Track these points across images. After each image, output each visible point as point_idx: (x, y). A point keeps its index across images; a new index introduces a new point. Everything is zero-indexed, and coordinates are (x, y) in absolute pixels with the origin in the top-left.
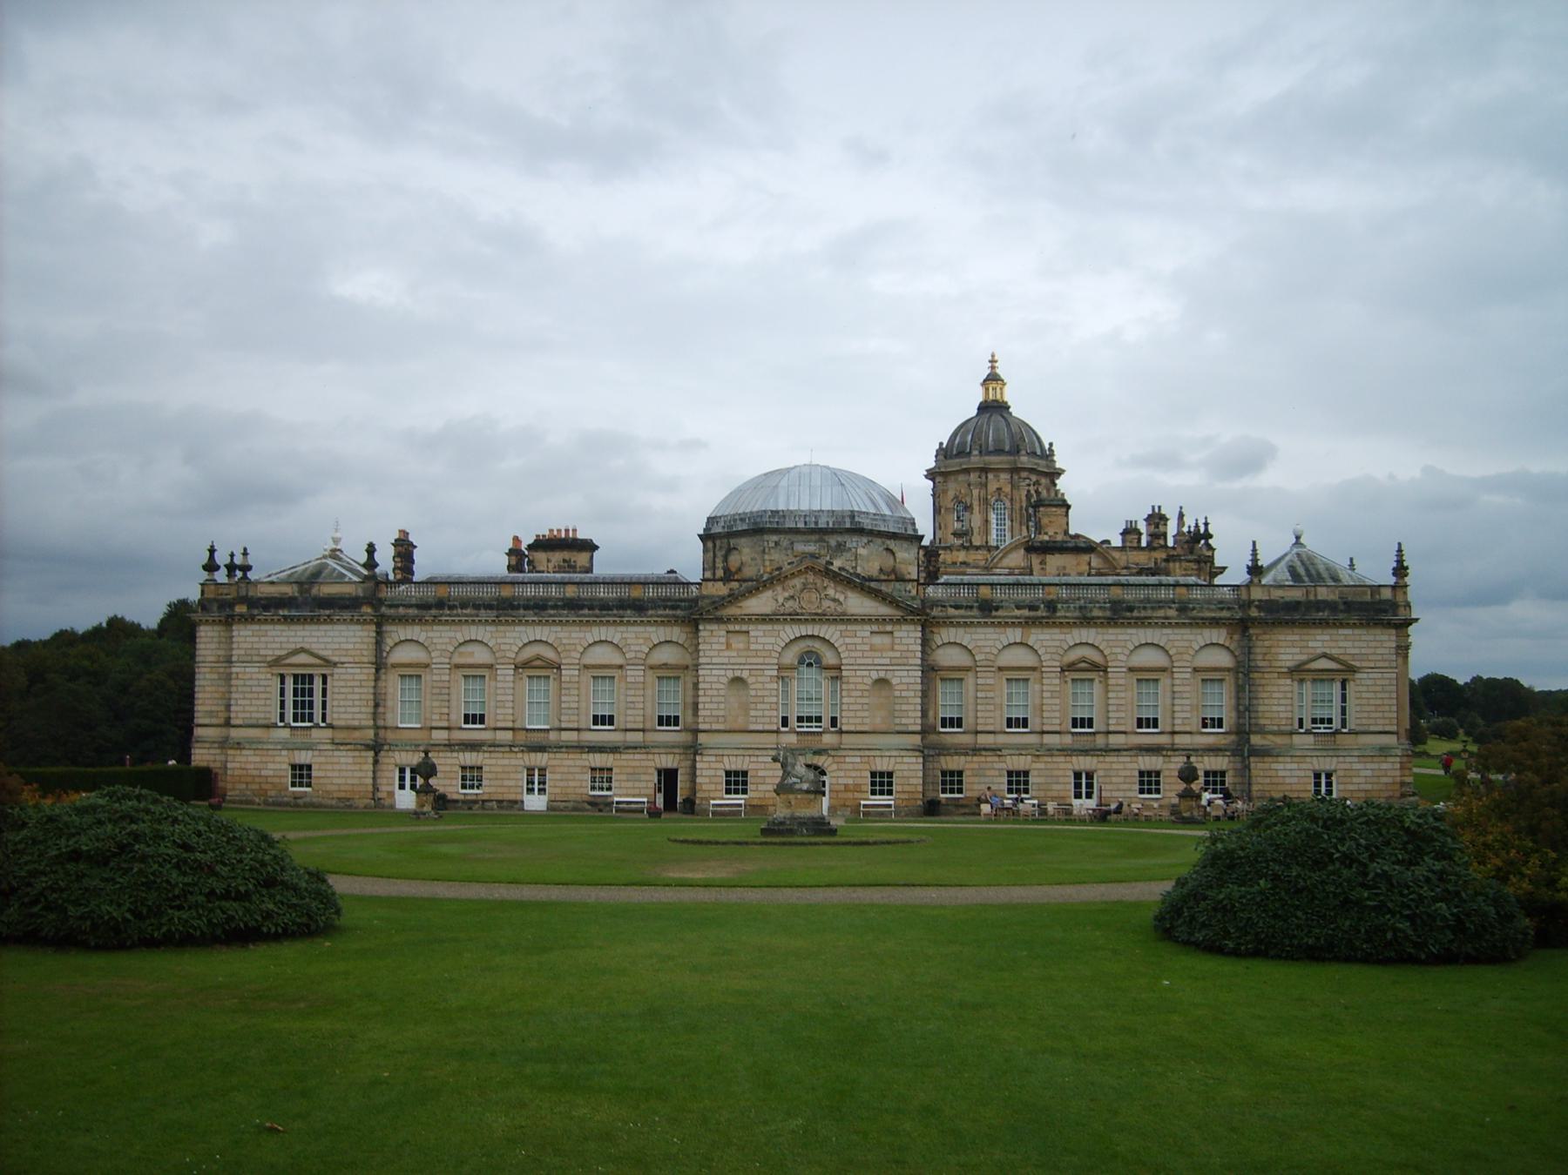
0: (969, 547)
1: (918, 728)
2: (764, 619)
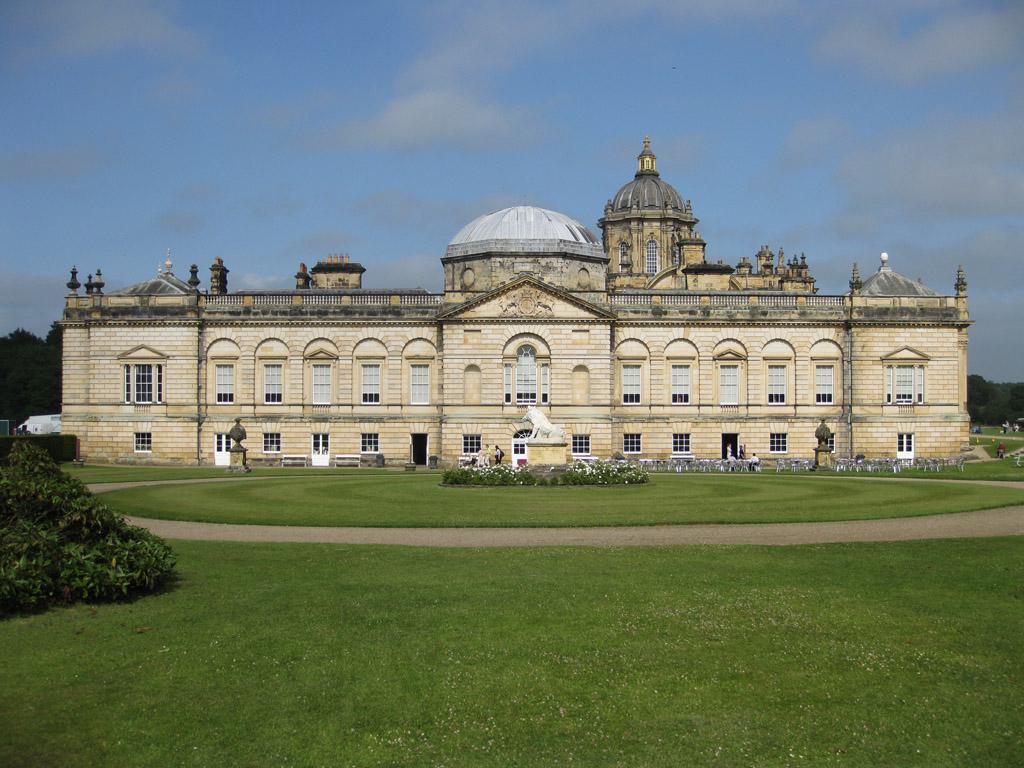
0: (630, 274)
1: (608, 402)
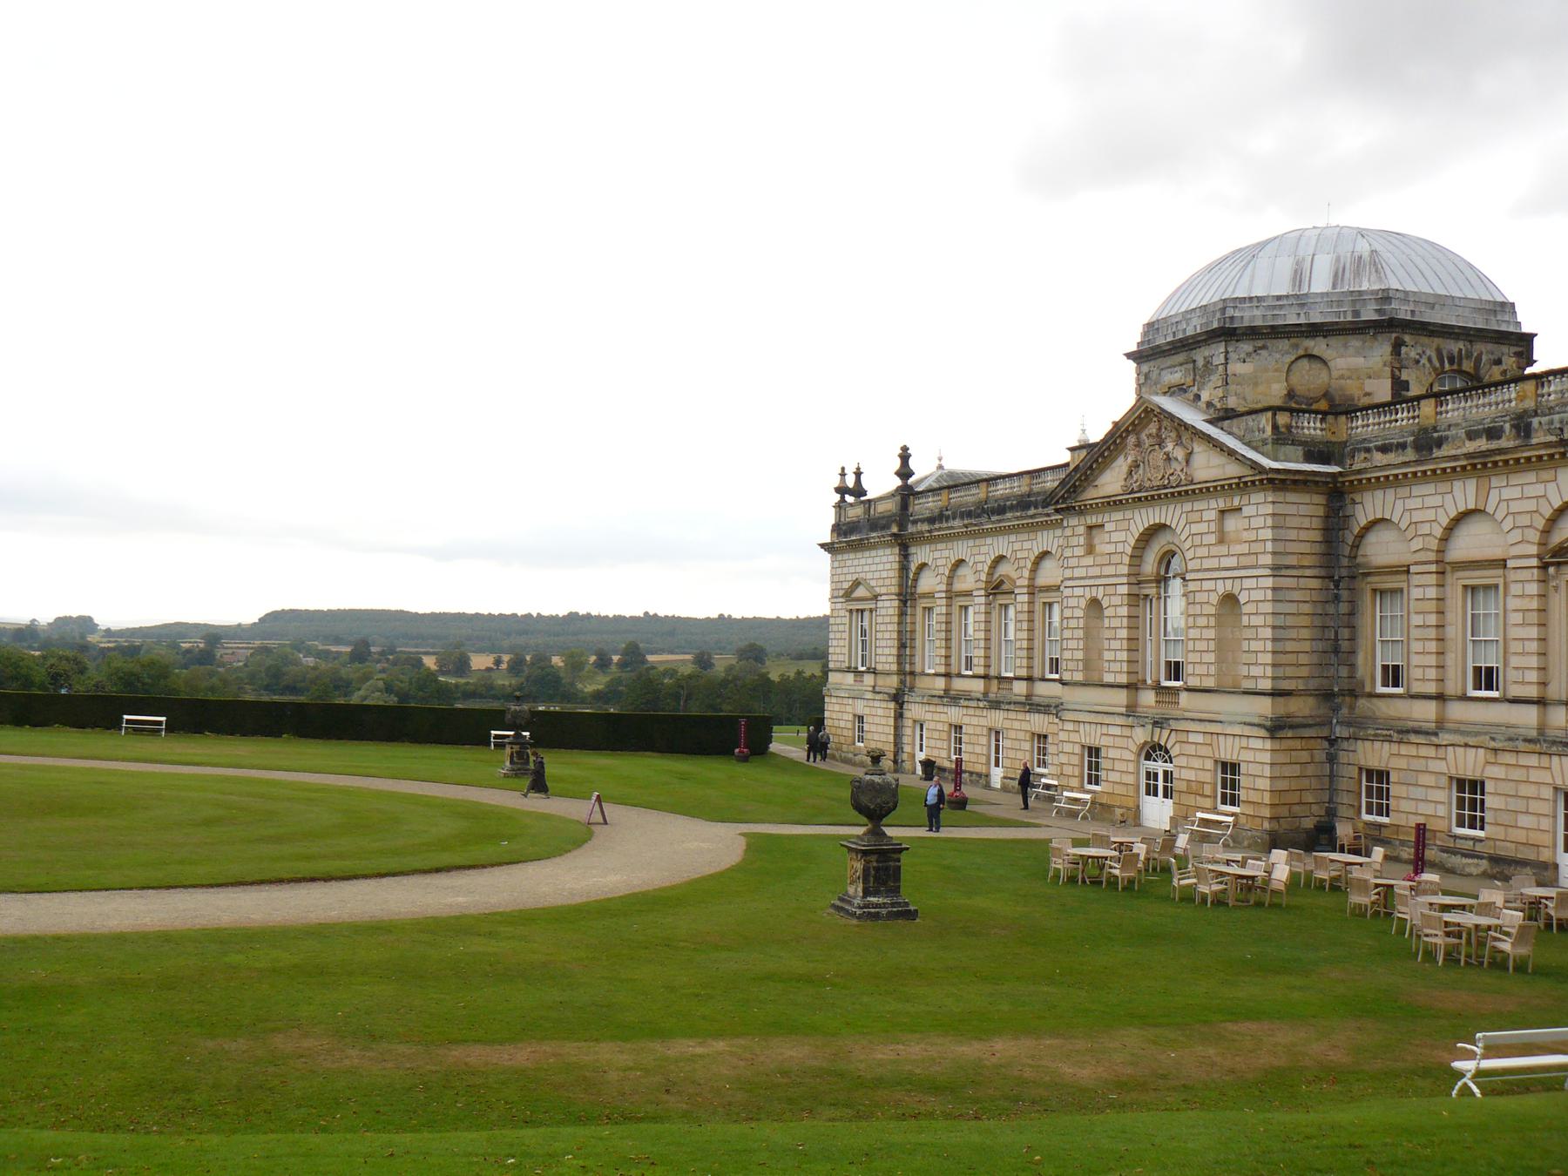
1: (1266, 685)
2: (1113, 504)
